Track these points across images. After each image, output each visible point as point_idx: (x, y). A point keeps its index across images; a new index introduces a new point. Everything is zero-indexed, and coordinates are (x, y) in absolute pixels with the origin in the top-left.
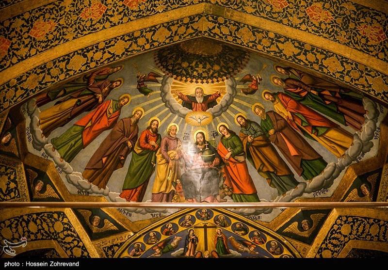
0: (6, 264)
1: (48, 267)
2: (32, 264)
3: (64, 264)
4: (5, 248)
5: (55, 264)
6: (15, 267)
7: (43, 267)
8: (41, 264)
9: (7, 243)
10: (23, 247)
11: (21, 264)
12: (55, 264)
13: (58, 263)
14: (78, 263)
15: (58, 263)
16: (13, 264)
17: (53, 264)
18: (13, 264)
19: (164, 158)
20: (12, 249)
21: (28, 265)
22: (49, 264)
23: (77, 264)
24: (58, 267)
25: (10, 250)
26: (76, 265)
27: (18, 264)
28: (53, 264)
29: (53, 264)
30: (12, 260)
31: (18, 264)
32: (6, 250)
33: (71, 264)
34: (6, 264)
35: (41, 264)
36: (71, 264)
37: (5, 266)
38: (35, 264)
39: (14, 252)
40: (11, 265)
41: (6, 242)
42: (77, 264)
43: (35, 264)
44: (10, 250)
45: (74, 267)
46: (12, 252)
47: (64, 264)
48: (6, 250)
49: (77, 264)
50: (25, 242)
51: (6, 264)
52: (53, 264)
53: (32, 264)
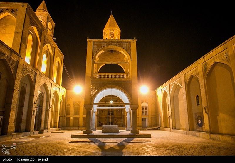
0: (4, 160)
2: (19, 160)
3: (39, 159)
5: (34, 160)
8: (25, 160)
11: (13, 160)
12: (34, 160)
13: (35, 159)
14: (47, 159)
15: (35, 159)
16: (8, 160)
17: (32, 159)
18: (8, 160)
19: (59, 56)
21: (17, 160)
22: (30, 159)
23: (47, 159)
26: (46, 160)
27: (11, 160)
29: (32, 160)
31: (11, 160)
33: (43, 160)
34: (4, 160)
35: (25, 160)
36: (43, 160)
37: (3, 160)
38: (21, 160)
40: (7, 160)
42: (47, 160)
43: (21, 160)
47: (39, 159)
49: (47, 159)
51: (4, 160)
52: (32, 160)
53: (19, 160)
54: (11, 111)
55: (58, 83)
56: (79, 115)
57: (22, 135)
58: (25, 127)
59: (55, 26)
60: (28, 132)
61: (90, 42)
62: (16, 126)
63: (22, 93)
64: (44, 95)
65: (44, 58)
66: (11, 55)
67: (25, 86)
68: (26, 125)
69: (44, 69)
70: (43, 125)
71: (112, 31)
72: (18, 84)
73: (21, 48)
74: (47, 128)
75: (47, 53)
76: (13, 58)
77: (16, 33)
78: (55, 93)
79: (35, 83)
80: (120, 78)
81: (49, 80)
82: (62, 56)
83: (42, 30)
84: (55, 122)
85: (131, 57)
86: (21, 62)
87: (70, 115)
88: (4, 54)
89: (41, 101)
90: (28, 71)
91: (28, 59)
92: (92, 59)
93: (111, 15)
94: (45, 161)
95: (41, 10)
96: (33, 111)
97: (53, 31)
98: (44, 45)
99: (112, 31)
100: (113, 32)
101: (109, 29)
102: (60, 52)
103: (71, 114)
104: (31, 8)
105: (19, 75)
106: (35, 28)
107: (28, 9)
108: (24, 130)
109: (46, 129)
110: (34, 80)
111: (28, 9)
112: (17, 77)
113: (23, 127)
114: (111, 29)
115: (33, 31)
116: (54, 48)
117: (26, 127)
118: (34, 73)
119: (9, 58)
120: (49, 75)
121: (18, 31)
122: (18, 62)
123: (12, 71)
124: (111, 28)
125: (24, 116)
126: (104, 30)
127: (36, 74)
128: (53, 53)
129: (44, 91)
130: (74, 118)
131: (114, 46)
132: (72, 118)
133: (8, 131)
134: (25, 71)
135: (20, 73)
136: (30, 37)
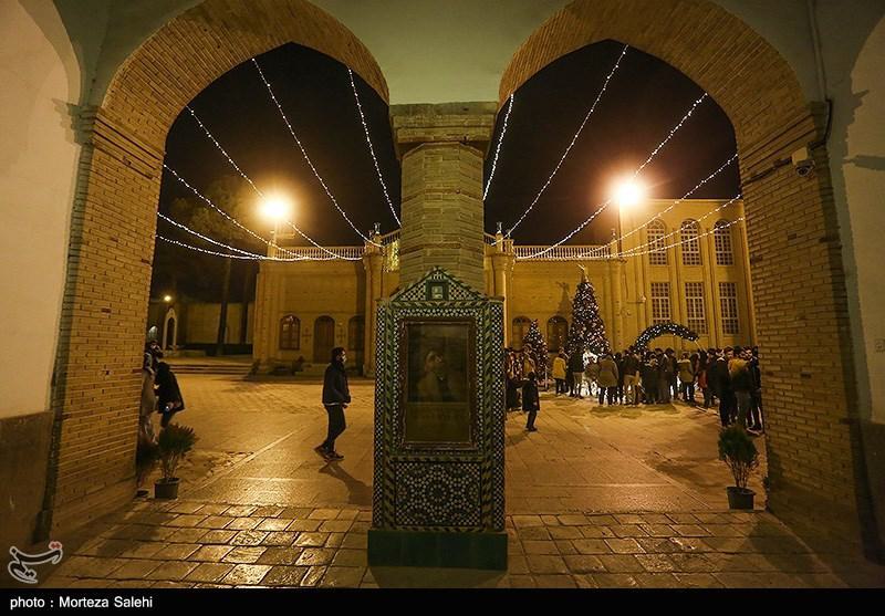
0: (15, 603)
2: (74, 603)
4: (14, 566)
6: (34, 610)
9: (18, 555)
10: (54, 563)
11: (48, 603)
16: (29, 603)
17: (119, 602)
18: (29, 603)
20: (29, 567)
25: (23, 570)
27: (41, 603)
28: (119, 602)
30: (28, 592)
31: (41, 603)
32: (16, 570)
34: (14, 603)
37: (12, 606)
39: (32, 574)
40: (25, 604)
41: (14, 551)
44: (23, 570)
46: (28, 574)
48: (16, 570)
50: (57, 553)
51: (15, 603)
53: (74, 603)
94: (144, 610)
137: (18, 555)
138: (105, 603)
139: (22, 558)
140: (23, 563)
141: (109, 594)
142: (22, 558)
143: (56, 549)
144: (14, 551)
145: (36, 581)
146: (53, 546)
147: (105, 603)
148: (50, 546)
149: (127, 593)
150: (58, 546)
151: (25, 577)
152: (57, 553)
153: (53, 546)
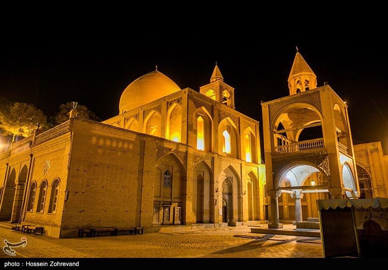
0: (6, 264)
1: (48, 267)
2: (32, 264)
3: (64, 264)
5: (55, 264)
6: (15, 268)
7: (43, 268)
8: (41, 264)
9: (8, 243)
11: (21, 264)
12: (55, 264)
13: (58, 263)
14: (78, 263)
15: (58, 263)
16: (13, 264)
17: (53, 264)
18: (13, 264)
21: (28, 265)
22: (49, 264)
23: (77, 264)
24: (58, 267)
25: (10, 250)
26: (76, 265)
27: (18, 264)
29: (53, 264)
30: (12, 260)
31: (18, 264)
32: (7, 250)
33: (71, 264)
34: (6, 264)
35: (41, 264)
36: (71, 264)
37: (5, 266)
38: (35, 264)
39: (14, 252)
40: (11, 265)
41: (6, 242)
42: (77, 264)
43: (35, 264)
44: (10, 250)
45: (74, 267)
46: (11, 252)
47: (64, 264)
49: (77, 264)
50: (25, 242)
51: (6, 264)
52: (53, 264)
53: (32, 264)
54: (187, 202)
55: (254, 161)
56: (306, 201)
57: (204, 226)
58: (209, 218)
59: (235, 91)
60: (212, 223)
61: (265, 107)
62: (197, 216)
63: (200, 182)
64: (232, 180)
65: (226, 134)
66: (178, 147)
67: (202, 174)
68: (210, 216)
69: (227, 149)
70: (236, 217)
71: (302, 77)
72: (191, 175)
73: (189, 136)
74: (242, 220)
75: (229, 129)
76: (180, 150)
77: (183, 122)
78: (251, 174)
79: (213, 168)
80: (320, 147)
81: (235, 160)
82: (254, 124)
83: (213, 106)
84: (258, 212)
85: (322, 115)
86: (191, 151)
87: (282, 202)
88: (170, 149)
89: (230, 187)
90: (202, 158)
91: (200, 145)
92: (270, 129)
93: (298, 54)
95: (132, 134)
96: (215, 201)
97: (234, 98)
98: (219, 122)
99: (302, 77)
100: (299, 79)
101: (293, 77)
102: (247, 119)
103: (283, 201)
104: (193, 91)
105: (191, 164)
106: (203, 108)
107: (190, 94)
108: (208, 222)
109: (241, 221)
110: (212, 166)
111: (190, 94)
112: (188, 167)
113: (206, 217)
114: (296, 77)
115: (202, 112)
116: (237, 120)
117: (210, 218)
118: (210, 158)
119: (177, 151)
120: (237, 154)
121: (184, 120)
122: (187, 153)
123: (182, 163)
124: (296, 75)
125: (206, 206)
126: (288, 81)
127: (213, 158)
128: (238, 126)
129: (232, 175)
130: (290, 207)
131: (296, 104)
132: (286, 207)
133: (187, 221)
134: (198, 159)
135: (191, 163)
136: (200, 119)
137: (8, 243)
138: (46, 264)
139: (9, 245)
140: (10, 247)
141: (48, 260)
142: (9, 245)
143: (24, 241)
144: (6, 242)
145: (15, 255)
146: (23, 239)
147: (46, 264)
148: (21, 239)
149: (55, 260)
150: (25, 239)
151: (10, 253)
152: (25, 242)
153: (23, 239)
